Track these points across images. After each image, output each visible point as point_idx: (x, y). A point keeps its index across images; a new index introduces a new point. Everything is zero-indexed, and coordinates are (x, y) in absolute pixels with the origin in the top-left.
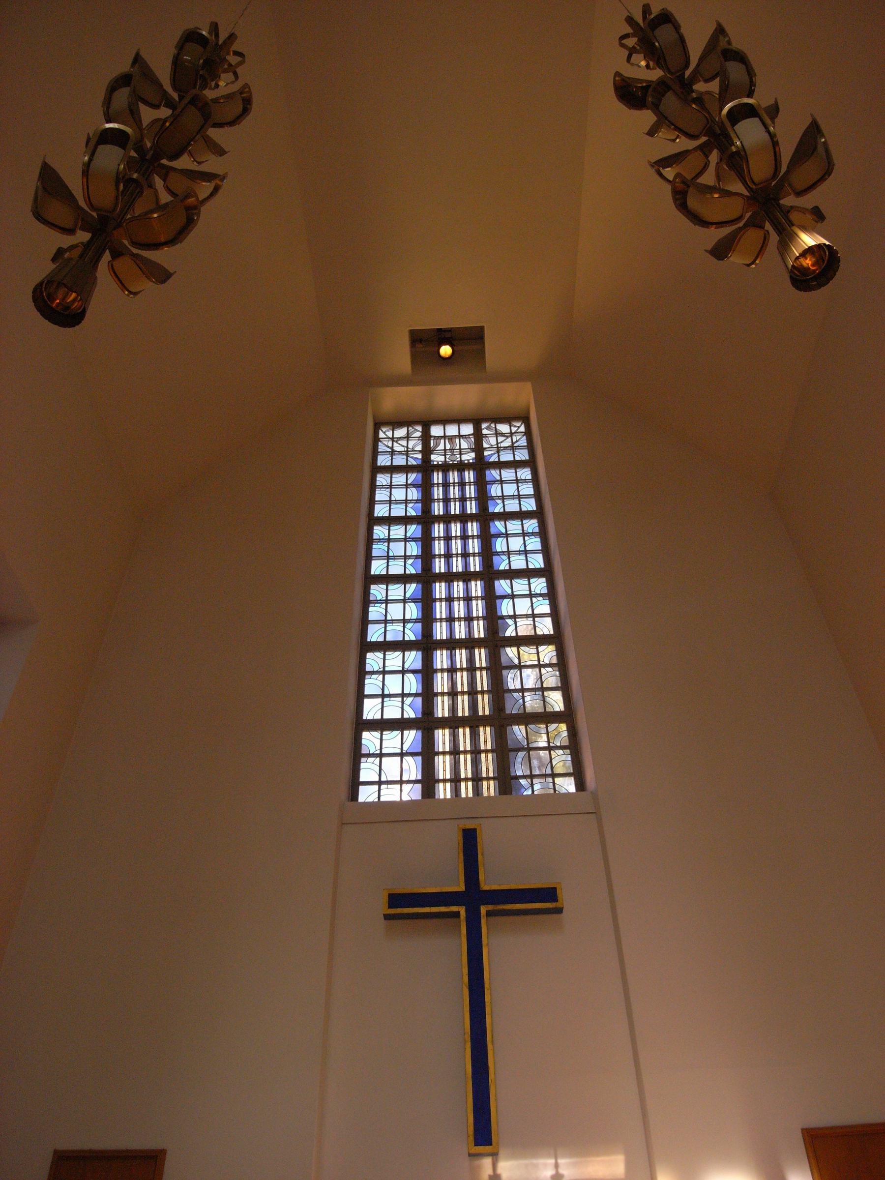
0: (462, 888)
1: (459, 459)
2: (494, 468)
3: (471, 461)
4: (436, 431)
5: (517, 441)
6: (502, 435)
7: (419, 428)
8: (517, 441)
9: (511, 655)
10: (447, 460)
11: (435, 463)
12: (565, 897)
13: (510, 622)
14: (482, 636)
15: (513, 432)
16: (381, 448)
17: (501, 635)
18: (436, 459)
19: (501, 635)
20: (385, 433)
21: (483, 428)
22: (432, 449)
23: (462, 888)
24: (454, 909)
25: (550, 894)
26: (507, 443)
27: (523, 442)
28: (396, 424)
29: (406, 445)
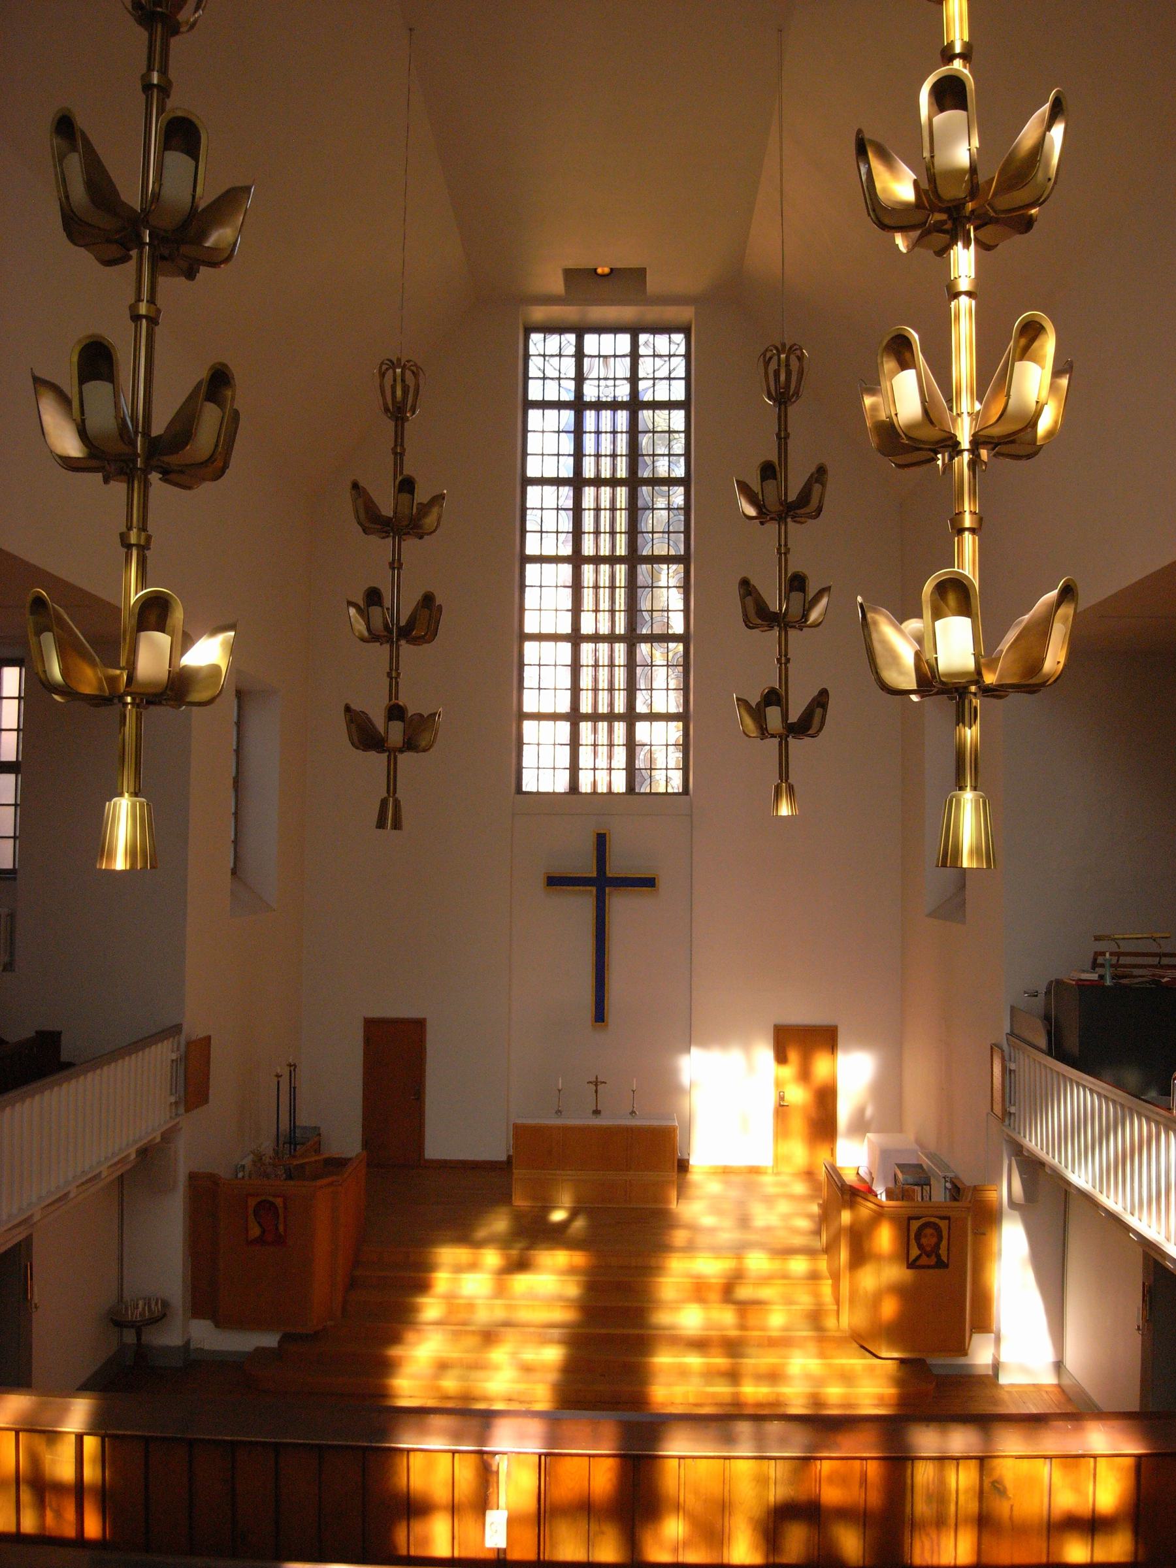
0: (595, 875)
1: (612, 395)
2: (648, 409)
3: (625, 399)
4: (591, 342)
5: (674, 369)
6: (660, 356)
7: (571, 338)
8: (674, 369)
9: (645, 652)
10: (601, 395)
11: (588, 400)
12: (661, 883)
13: (646, 615)
14: (622, 632)
15: (672, 353)
16: (533, 371)
17: (638, 632)
18: (590, 393)
19: (638, 632)
20: (536, 338)
21: (640, 343)
22: (585, 375)
23: (595, 875)
24: (589, 888)
25: (649, 883)
26: (663, 373)
27: (681, 372)
28: (549, 329)
29: (558, 369)
